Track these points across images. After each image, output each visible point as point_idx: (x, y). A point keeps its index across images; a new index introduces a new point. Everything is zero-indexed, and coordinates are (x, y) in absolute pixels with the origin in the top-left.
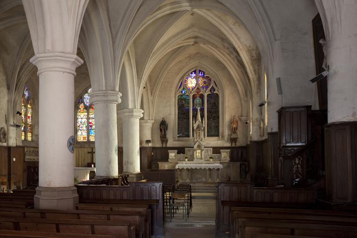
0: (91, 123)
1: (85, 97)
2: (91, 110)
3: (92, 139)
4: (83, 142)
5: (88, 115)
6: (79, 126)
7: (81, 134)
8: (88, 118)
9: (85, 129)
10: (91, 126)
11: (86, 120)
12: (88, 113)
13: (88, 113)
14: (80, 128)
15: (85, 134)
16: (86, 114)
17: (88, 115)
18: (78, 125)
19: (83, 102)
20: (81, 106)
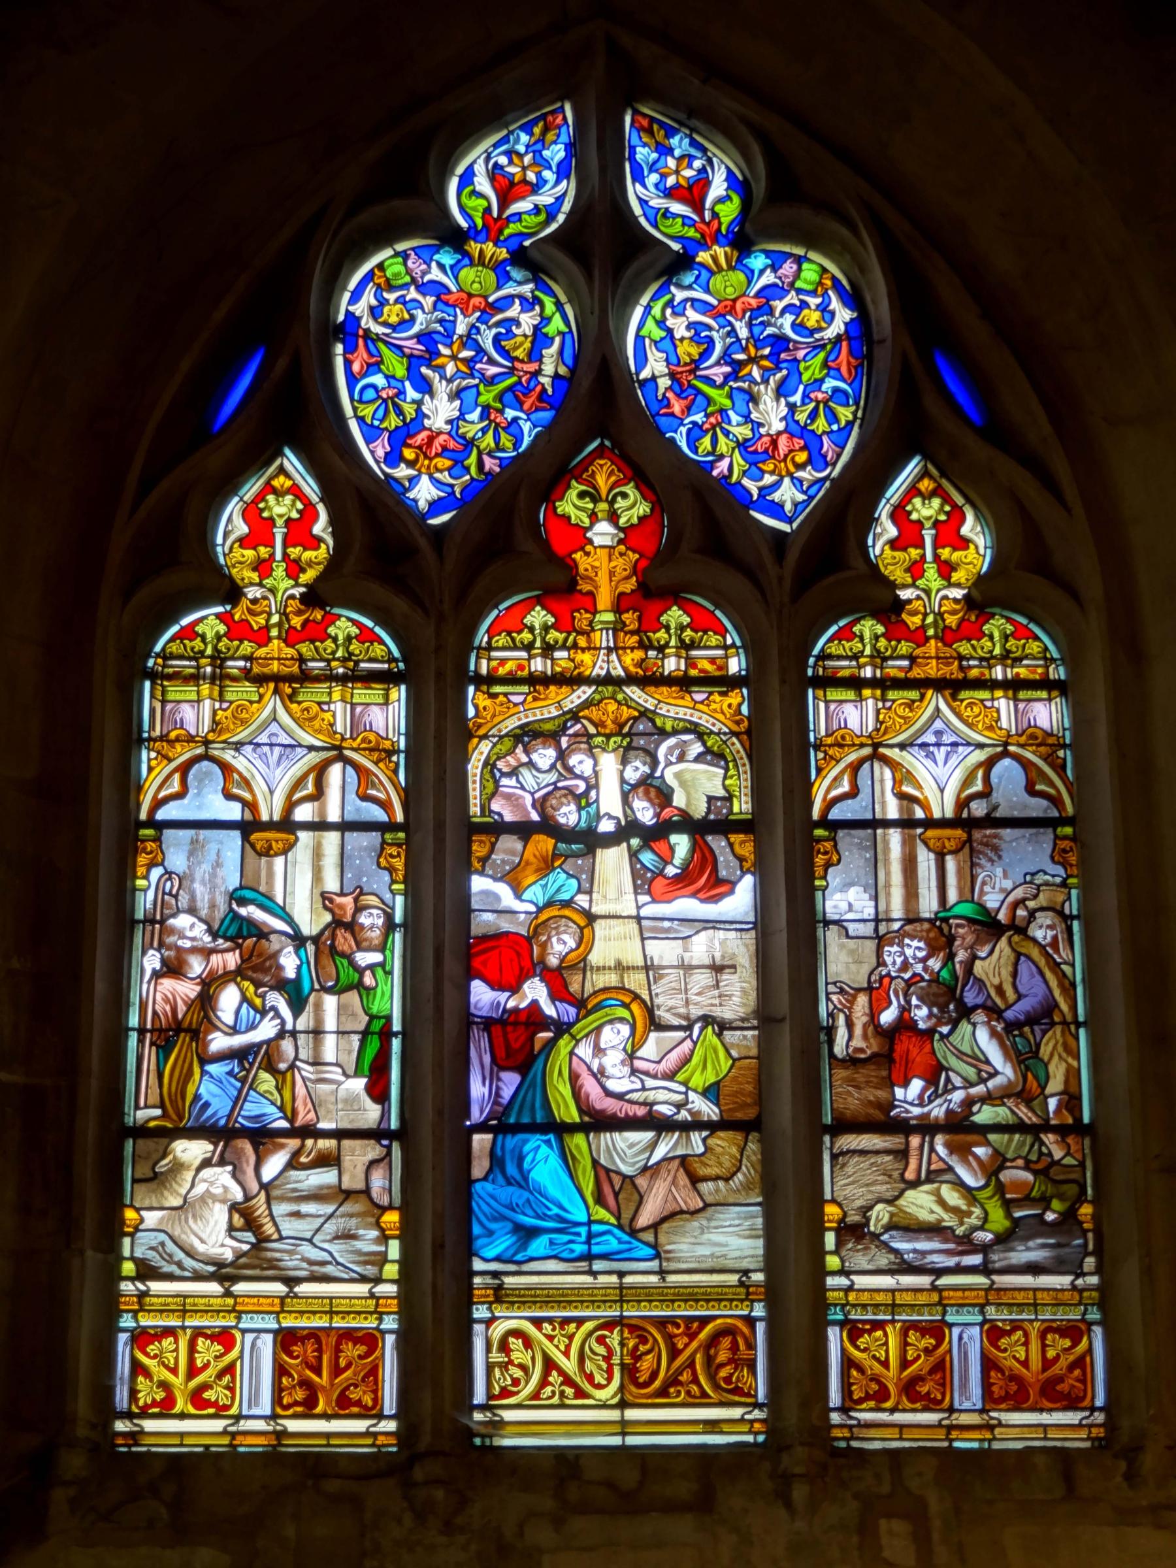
0: (513, 957)
1: (355, 302)
2: (513, 639)
3: (549, 1391)
4: (315, 1467)
5: (438, 741)
6: (184, 1032)
7: (214, 1236)
8: (435, 833)
9: (346, 1098)
10: (521, 1043)
11: (386, 898)
12: (437, 679)
13: (437, 679)
14: (212, 1090)
15: (348, 1270)
16: (389, 715)
17: (438, 741)
18: (155, 992)
19: (301, 416)
20: (267, 525)
